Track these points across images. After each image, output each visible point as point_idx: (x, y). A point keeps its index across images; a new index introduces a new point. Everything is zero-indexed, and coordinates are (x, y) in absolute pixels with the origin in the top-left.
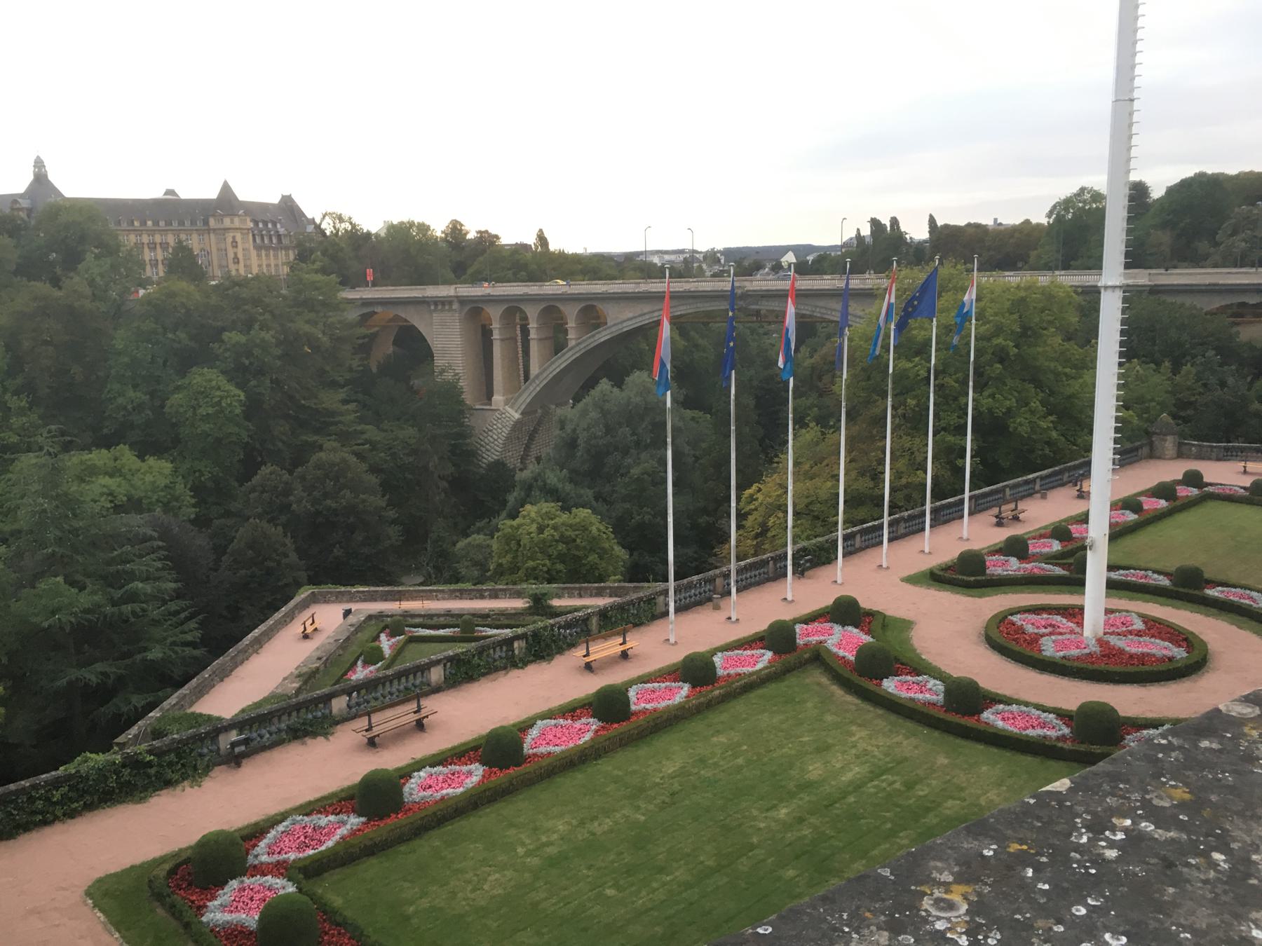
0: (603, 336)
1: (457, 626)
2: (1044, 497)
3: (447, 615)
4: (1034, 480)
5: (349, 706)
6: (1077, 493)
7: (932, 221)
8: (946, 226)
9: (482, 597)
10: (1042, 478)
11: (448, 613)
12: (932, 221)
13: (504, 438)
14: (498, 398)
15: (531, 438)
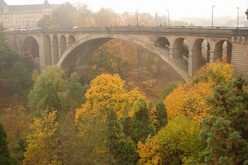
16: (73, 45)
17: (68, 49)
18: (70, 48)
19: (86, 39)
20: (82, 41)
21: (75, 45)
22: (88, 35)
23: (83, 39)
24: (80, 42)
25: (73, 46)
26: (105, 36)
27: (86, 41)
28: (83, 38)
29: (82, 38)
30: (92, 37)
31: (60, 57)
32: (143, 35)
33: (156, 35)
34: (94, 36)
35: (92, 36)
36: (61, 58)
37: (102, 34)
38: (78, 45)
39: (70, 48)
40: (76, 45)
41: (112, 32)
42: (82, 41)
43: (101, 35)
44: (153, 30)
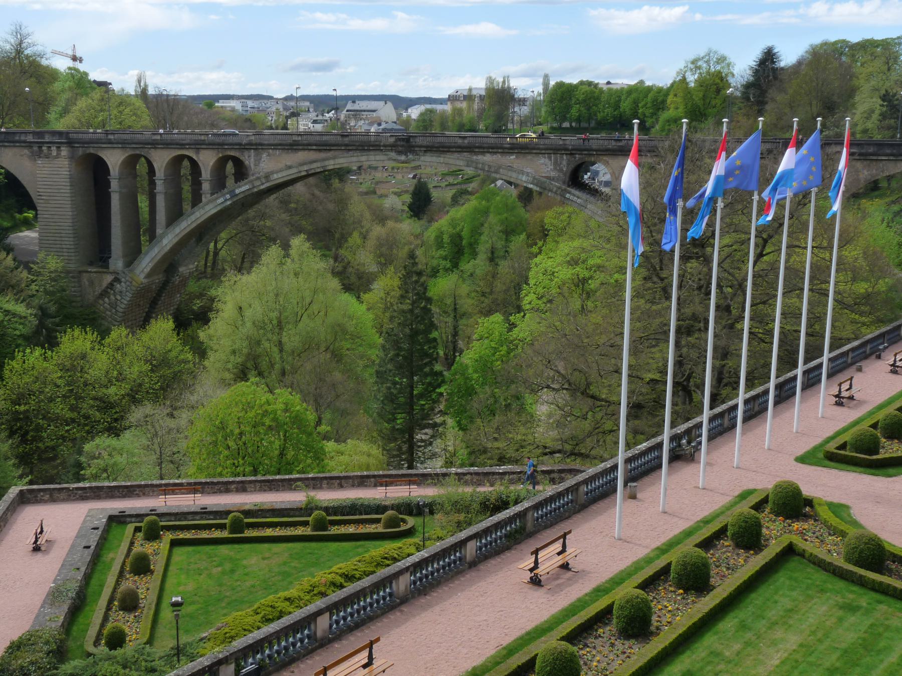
0: (243, 188)
1: (222, 527)
2: (860, 370)
3: (205, 513)
4: (848, 351)
5: (331, 626)
6: (890, 368)
7: (546, 77)
8: (560, 85)
9: (228, 491)
10: (853, 350)
11: (204, 513)
12: (546, 77)
13: (123, 306)
14: (117, 262)
15: (154, 303)
16: (240, 187)
17: (207, 204)
18: (221, 200)
19: (306, 168)
20: (280, 175)
21: (247, 187)
22: (312, 155)
23: (290, 167)
24: (275, 176)
25: (237, 191)
26: (389, 159)
27: (304, 174)
28: (289, 164)
29: (281, 165)
30: (332, 162)
31: (159, 231)
32: (529, 157)
33: (569, 156)
34: (341, 161)
35: (334, 158)
36: (163, 236)
37: (378, 152)
38: (268, 185)
39: (221, 200)
40: (254, 187)
41: (421, 146)
42: (284, 174)
43: (372, 158)
44: (565, 145)
